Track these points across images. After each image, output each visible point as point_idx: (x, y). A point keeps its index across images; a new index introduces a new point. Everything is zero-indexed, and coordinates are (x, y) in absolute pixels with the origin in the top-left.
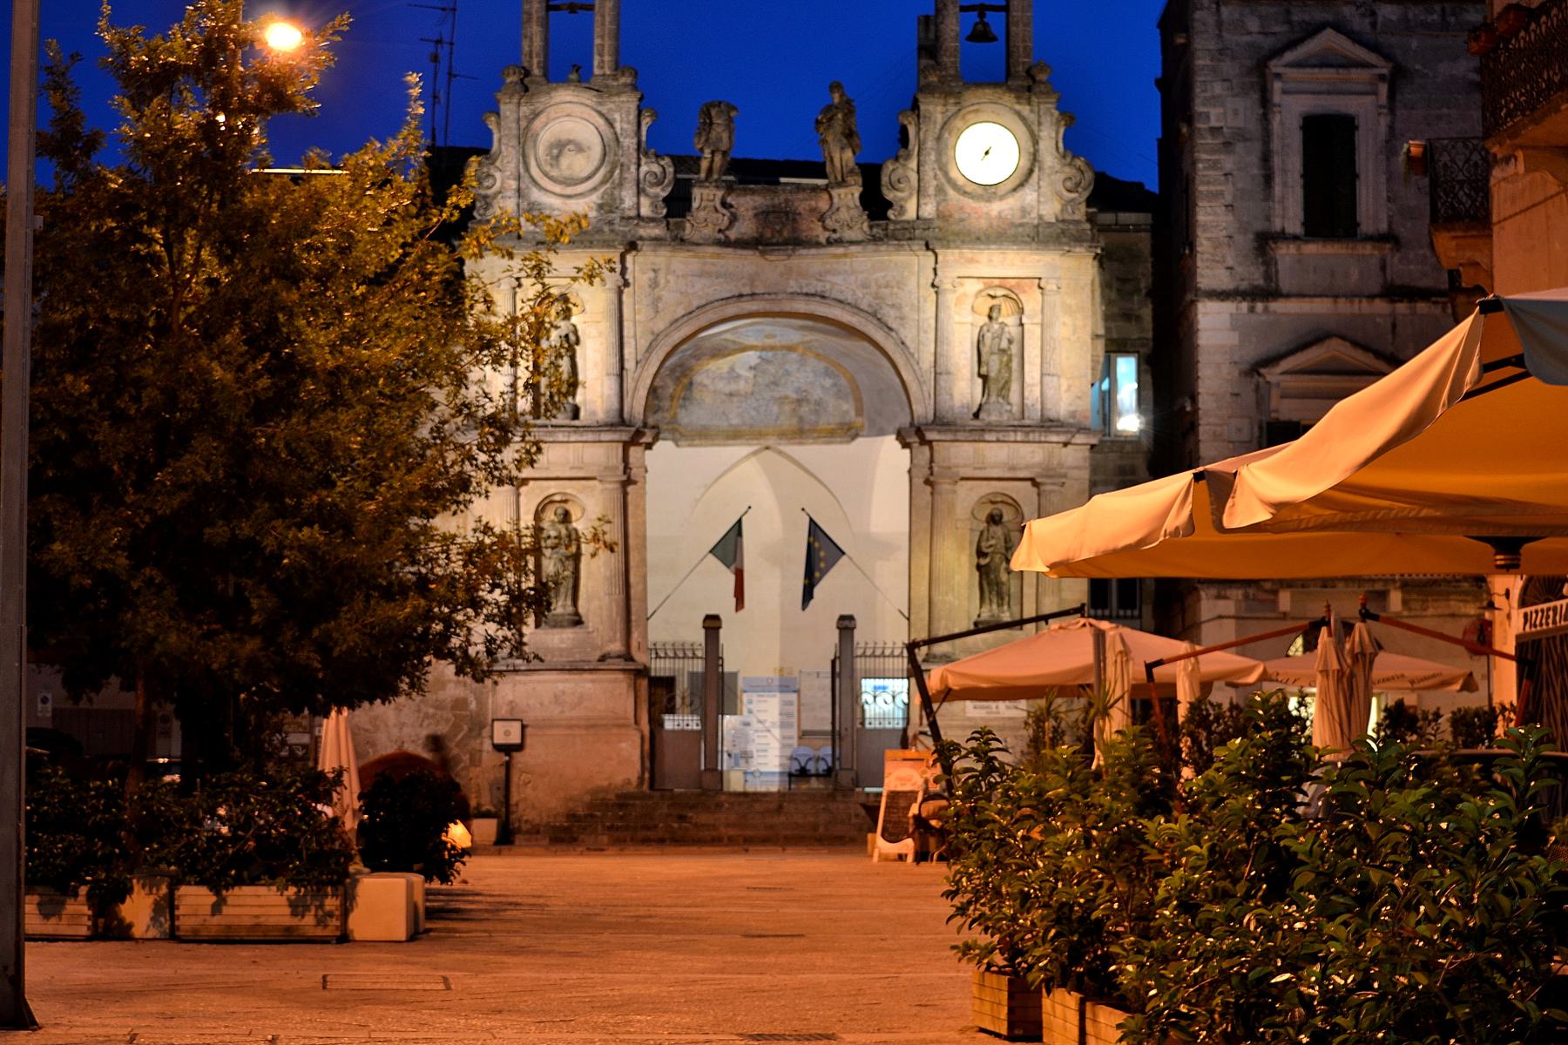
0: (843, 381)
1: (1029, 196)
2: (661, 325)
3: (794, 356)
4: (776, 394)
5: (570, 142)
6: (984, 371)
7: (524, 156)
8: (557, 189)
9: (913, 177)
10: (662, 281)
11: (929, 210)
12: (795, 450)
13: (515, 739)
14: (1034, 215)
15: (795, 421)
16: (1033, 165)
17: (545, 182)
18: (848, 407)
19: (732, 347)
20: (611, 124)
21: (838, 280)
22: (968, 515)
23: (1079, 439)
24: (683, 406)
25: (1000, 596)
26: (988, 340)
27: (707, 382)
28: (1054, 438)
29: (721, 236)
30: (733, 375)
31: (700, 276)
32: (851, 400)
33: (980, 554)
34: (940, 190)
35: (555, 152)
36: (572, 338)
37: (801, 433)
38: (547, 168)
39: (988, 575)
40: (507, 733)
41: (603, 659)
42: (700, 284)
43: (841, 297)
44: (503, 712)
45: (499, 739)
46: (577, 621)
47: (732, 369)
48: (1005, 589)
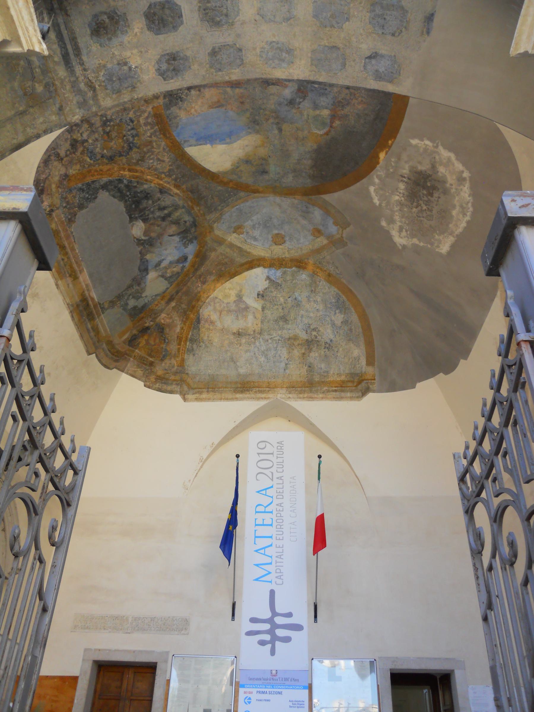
0: (354, 318)
3: (304, 276)
4: (286, 334)
12: (306, 407)
15: (304, 371)
18: (358, 352)
19: (240, 260)
24: (191, 351)
27: (214, 317)
30: (240, 308)
32: (363, 347)
37: (311, 385)
47: (240, 297)
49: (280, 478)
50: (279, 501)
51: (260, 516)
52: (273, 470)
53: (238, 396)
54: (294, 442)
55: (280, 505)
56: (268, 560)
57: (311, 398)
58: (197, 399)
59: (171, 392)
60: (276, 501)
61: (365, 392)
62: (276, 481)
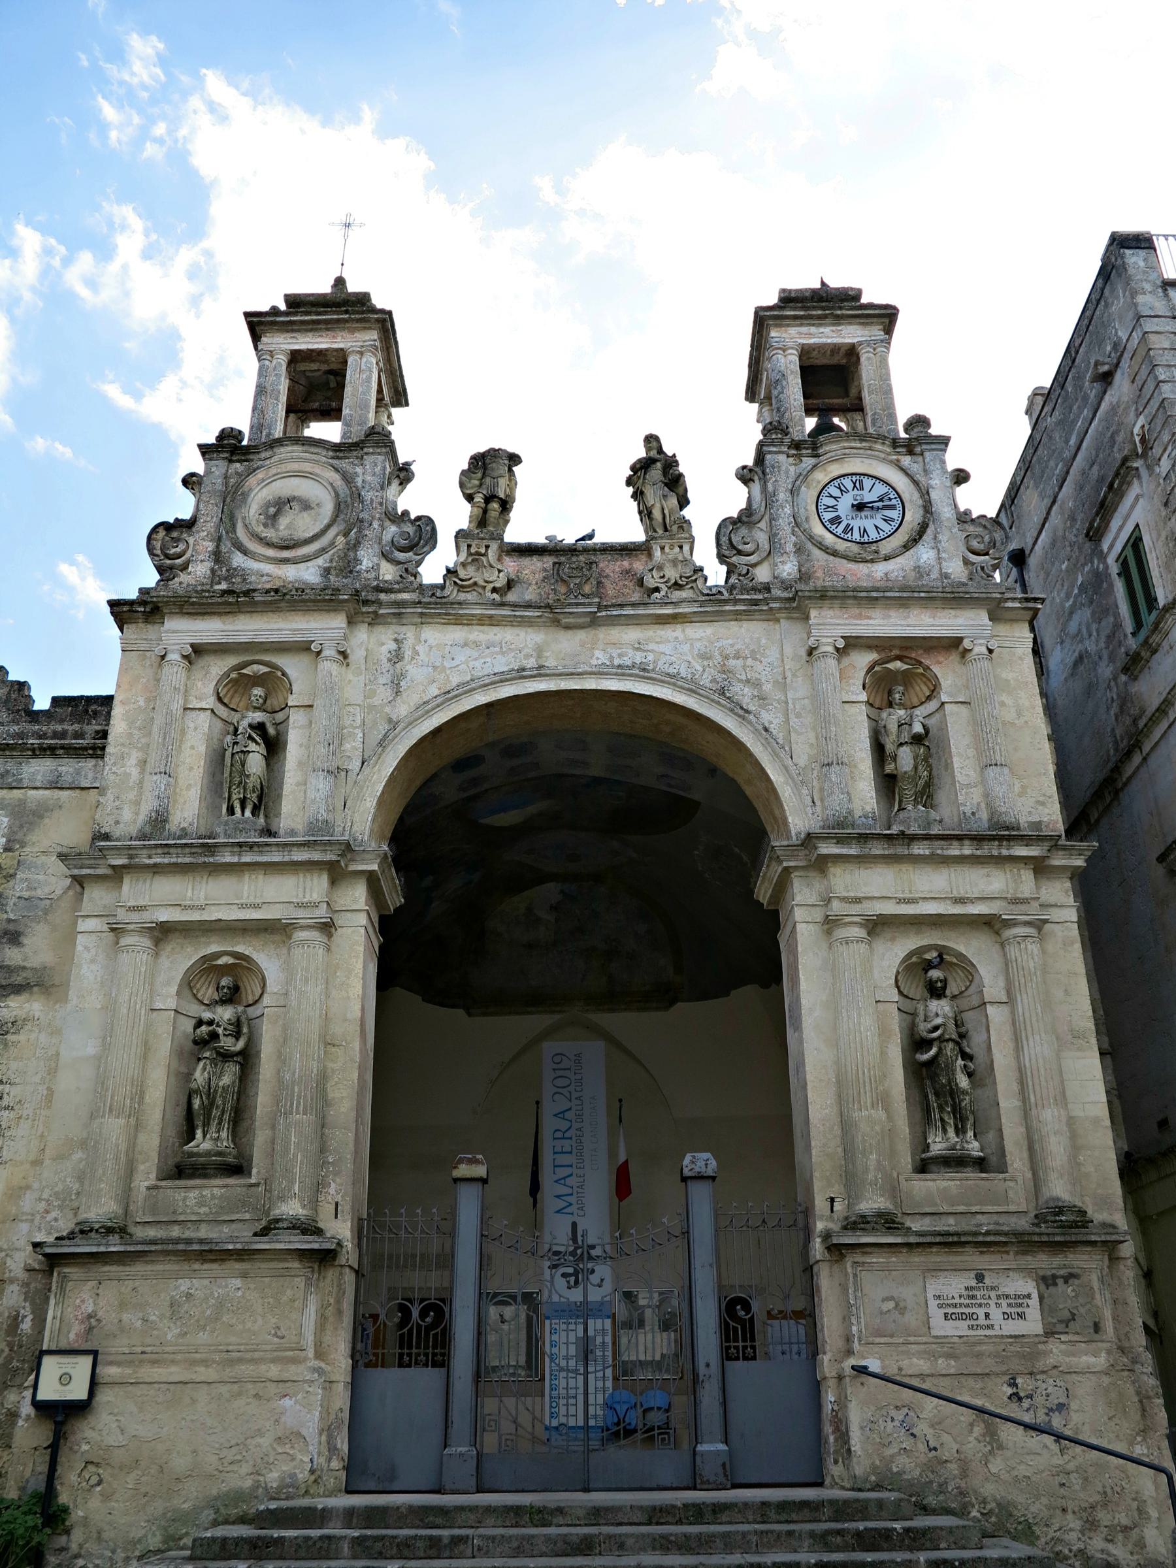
1: (924, 554)
2: (402, 710)
5: (294, 498)
6: (889, 768)
7: (232, 518)
8: (271, 553)
9: (762, 537)
10: (408, 654)
11: (788, 568)
13: (78, 1391)
14: (935, 575)
16: (924, 517)
17: (252, 546)
20: (348, 479)
21: (666, 648)
22: (893, 981)
23: (1058, 860)
25: (957, 1111)
26: (893, 727)
28: (1022, 851)
29: (495, 596)
31: (466, 645)
33: (916, 1043)
34: (799, 550)
35: (272, 510)
36: (271, 731)
37: (613, 998)
38: (259, 529)
39: (933, 1078)
40: (65, 1379)
41: (264, 1232)
42: (461, 656)
43: (671, 671)
44: (72, 1338)
45: (49, 1390)
46: (238, 1169)
48: (966, 1101)
49: (578, 1098)
50: (578, 1125)
51: (558, 1143)
52: (571, 1088)
53: (529, 1009)
54: (594, 1051)
55: (579, 1129)
56: (569, 1191)
57: (612, 1010)
58: (485, 1014)
59: (453, 1006)
60: (575, 1126)
61: (672, 1002)
62: (575, 1102)
